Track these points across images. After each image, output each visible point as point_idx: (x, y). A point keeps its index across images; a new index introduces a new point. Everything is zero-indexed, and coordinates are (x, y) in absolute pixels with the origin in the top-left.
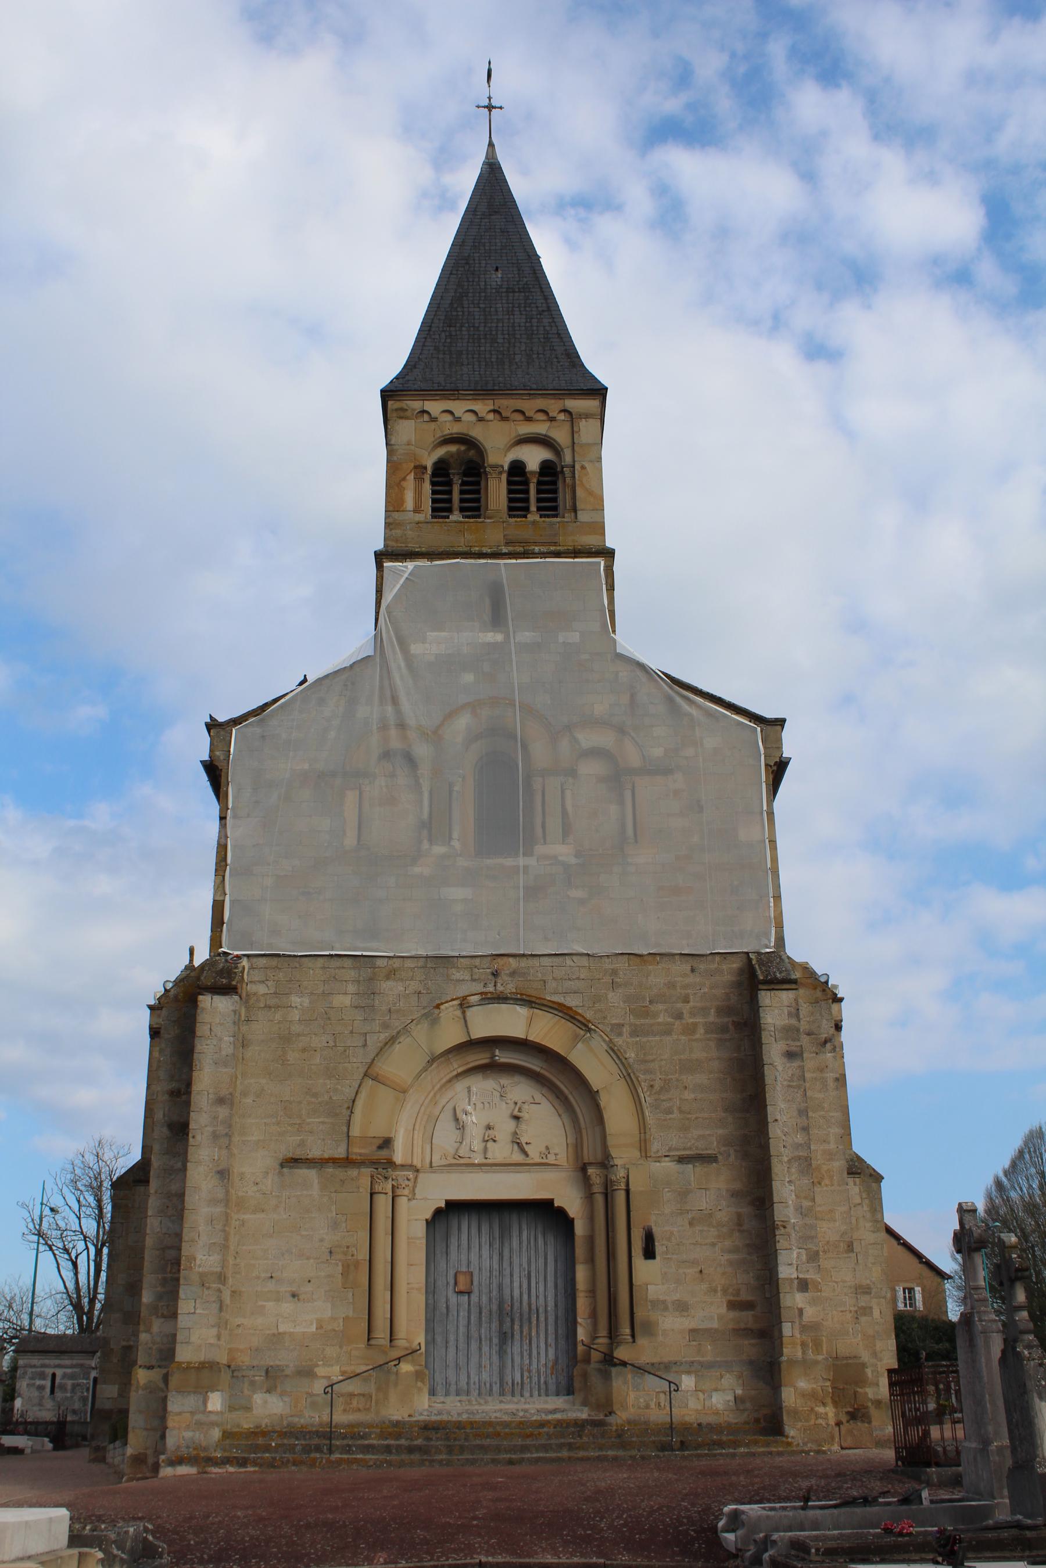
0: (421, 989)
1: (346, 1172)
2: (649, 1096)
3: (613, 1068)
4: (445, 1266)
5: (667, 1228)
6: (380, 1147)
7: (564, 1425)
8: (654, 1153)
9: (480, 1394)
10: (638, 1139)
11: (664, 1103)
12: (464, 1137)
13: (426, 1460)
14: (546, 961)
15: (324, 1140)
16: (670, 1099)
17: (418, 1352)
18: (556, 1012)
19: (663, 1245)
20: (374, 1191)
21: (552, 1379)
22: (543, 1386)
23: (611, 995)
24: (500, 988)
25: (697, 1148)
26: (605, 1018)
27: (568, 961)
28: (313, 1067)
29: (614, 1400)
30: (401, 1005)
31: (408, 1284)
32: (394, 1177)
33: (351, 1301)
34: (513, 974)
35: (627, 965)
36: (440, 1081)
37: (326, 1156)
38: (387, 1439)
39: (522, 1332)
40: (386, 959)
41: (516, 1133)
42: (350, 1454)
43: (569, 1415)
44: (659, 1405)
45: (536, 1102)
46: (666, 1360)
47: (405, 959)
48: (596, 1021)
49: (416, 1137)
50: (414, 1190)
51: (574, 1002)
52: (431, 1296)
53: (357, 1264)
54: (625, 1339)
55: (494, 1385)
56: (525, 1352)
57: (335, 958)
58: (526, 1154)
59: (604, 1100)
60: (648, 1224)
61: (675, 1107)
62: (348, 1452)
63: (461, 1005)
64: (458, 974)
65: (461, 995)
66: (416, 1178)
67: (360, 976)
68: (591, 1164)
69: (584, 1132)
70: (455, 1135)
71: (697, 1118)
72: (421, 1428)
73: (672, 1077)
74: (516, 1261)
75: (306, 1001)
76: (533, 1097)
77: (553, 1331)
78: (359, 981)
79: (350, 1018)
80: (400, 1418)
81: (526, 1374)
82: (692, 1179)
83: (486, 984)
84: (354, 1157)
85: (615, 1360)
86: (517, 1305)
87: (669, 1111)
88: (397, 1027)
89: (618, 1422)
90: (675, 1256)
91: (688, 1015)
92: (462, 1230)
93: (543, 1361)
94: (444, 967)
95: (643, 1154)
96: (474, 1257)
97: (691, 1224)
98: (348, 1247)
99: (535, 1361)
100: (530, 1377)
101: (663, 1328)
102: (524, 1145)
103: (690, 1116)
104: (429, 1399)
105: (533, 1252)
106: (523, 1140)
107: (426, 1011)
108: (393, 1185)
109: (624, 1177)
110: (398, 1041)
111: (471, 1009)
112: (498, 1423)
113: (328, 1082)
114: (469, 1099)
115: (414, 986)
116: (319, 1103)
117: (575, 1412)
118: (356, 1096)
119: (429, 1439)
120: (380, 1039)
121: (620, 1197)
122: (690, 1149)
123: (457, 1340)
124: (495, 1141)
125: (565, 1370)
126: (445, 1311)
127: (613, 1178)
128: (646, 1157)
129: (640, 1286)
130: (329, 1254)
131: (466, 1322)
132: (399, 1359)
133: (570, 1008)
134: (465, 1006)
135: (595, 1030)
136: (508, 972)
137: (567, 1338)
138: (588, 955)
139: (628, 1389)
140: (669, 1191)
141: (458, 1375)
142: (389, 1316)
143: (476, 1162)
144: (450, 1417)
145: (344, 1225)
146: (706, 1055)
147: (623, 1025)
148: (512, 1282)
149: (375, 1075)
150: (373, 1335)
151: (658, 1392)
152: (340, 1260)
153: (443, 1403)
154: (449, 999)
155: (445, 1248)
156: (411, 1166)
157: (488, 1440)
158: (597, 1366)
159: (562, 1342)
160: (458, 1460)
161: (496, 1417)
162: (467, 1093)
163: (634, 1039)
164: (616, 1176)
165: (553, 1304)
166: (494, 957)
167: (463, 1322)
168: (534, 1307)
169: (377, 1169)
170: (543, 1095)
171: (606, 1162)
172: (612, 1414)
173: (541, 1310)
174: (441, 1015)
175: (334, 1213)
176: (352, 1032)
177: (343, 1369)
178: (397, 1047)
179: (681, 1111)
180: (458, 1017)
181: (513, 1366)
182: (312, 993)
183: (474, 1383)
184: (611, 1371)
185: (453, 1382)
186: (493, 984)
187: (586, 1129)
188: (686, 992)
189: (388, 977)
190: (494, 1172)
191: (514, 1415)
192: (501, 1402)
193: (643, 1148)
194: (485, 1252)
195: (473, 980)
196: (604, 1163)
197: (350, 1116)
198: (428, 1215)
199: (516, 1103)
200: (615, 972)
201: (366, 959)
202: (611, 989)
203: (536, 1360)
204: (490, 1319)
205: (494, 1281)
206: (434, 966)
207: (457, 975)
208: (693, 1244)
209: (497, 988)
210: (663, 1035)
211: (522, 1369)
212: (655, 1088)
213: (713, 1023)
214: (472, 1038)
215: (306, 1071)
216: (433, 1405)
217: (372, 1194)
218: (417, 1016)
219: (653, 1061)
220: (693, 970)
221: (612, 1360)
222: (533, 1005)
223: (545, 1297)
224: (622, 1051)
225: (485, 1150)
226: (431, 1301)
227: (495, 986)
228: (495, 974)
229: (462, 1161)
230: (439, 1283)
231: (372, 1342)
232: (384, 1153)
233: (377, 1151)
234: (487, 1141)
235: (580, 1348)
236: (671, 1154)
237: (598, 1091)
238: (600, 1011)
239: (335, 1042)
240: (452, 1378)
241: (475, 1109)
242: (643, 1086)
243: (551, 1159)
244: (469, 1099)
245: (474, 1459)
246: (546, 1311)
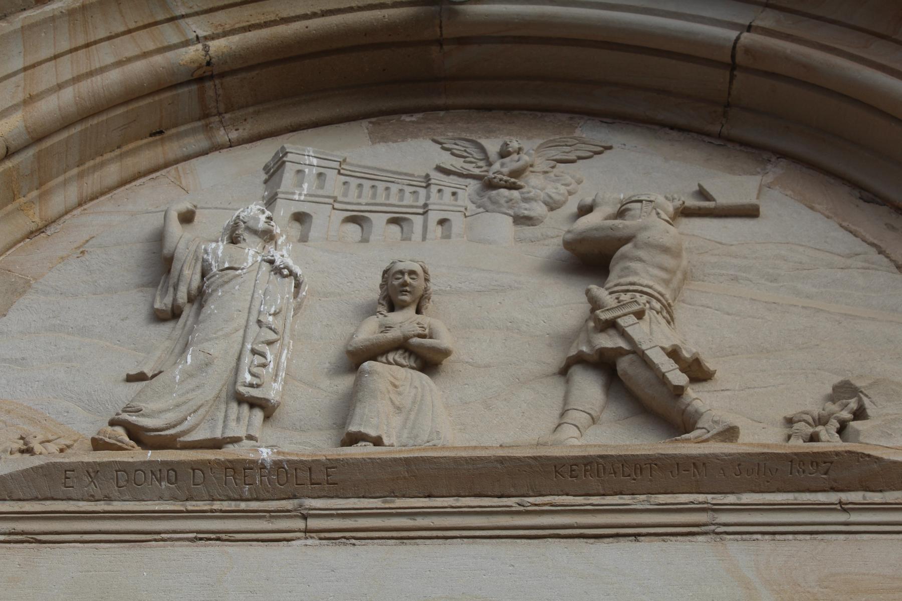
190: (403, 536)
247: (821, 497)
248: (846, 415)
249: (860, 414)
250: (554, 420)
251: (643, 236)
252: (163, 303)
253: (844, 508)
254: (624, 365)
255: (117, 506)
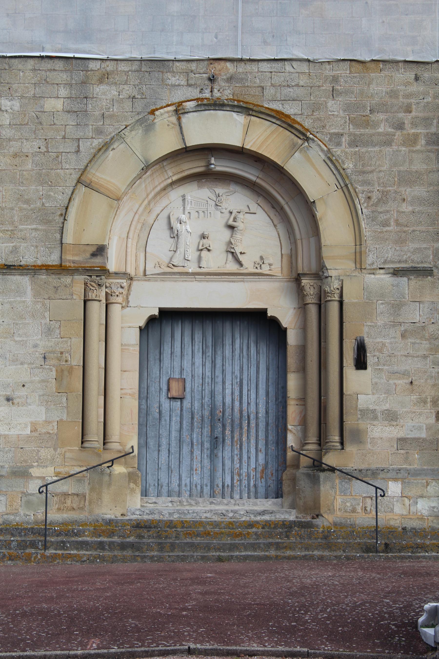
0: (135, 93)
1: (59, 279)
2: (365, 208)
3: (332, 180)
4: (158, 372)
5: (379, 340)
6: (94, 255)
7: (272, 526)
8: (370, 265)
9: (190, 496)
10: (354, 251)
11: (381, 215)
12: (179, 246)
13: (138, 556)
14: (265, 67)
15: (37, 247)
16: (388, 211)
17: (132, 455)
18: (274, 120)
19: (374, 356)
20: (87, 298)
21: (261, 482)
22: (252, 489)
23: (330, 103)
24: (217, 94)
25: (413, 261)
26: (324, 127)
27: (288, 67)
28: (24, 173)
29: (322, 503)
30: (115, 110)
31: (121, 389)
32: (108, 285)
33: (65, 405)
34: (230, 79)
35: (348, 72)
36: (153, 189)
37: (39, 263)
38: (100, 536)
39: (233, 437)
40: (99, 62)
41: (230, 243)
42: (66, 550)
43: (277, 516)
44: (366, 510)
45: (251, 212)
46: (373, 467)
47: (119, 62)
48: (314, 130)
49: (129, 245)
50: (127, 298)
51: (292, 110)
52: (144, 401)
53: (71, 370)
54: (333, 446)
55: (205, 487)
56: (235, 456)
57: (46, 60)
58: (241, 265)
59: (319, 212)
60: (361, 335)
61: (392, 220)
62: (63, 548)
63: (176, 111)
64: (174, 79)
65: (177, 101)
66: (130, 286)
67: (72, 79)
68: (304, 275)
69: (299, 242)
70: (170, 243)
71: (413, 231)
72: (133, 527)
73: (391, 188)
74: (228, 368)
75: (16, 105)
76: (248, 206)
77: (264, 437)
78: (71, 85)
79: (62, 123)
80: (113, 517)
81: (236, 477)
82: (407, 291)
83: (202, 89)
84: (68, 264)
85: (323, 465)
86: (228, 411)
87: (386, 224)
88: (110, 133)
89: (325, 524)
90: (386, 367)
91: (410, 125)
92: (175, 337)
93: (253, 466)
94: (159, 71)
95: (358, 266)
96: (187, 365)
97: (403, 336)
98: (62, 353)
99: (245, 465)
100: (240, 481)
101: (371, 436)
102: (239, 255)
103: (406, 229)
104: (142, 499)
105: (245, 360)
106: (238, 250)
107: (140, 117)
108: (106, 292)
109: (338, 289)
110: (112, 147)
111: (186, 115)
112: (208, 523)
113: (41, 188)
114: (184, 208)
115: (128, 90)
116: (31, 210)
117: (283, 514)
118: (69, 203)
119: (140, 537)
120: (94, 145)
121: (334, 308)
122: (406, 261)
123: (169, 444)
124: (209, 250)
125: (274, 474)
126: (157, 415)
127: (327, 289)
128: (361, 269)
129: (349, 395)
130: (43, 360)
131: (178, 427)
132: (112, 461)
133: (288, 116)
134: (180, 112)
135: (313, 140)
136: (225, 77)
137: (277, 443)
138: (309, 61)
139: (336, 493)
140: (382, 304)
141: (169, 477)
142: (102, 420)
143: (190, 271)
144: (161, 517)
145: (58, 331)
146: (426, 167)
147: (342, 135)
148: (224, 389)
149: (88, 182)
150: (86, 438)
151: (365, 497)
152: (54, 366)
153: (155, 503)
154: (164, 105)
155: (158, 355)
156: (125, 274)
157: (199, 538)
158: (305, 471)
159: (272, 447)
160: (169, 556)
161: (206, 518)
162: (181, 202)
163: (352, 150)
164: (330, 287)
165: (264, 411)
166: (212, 61)
167: (175, 426)
168: (245, 414)
169: (91, 276)
170: (259, 205)
171: (321, 273)
172: (319, 517)
173: (252, 416)
174: (155, 121)
175: (48, 320)
176: (64, 138)
177: (58, 470)
178: (111, 154)
179: (397, 223)
180: (173, 124)
181: (223, 470)
182: (22, 97)
183: (186, 485)
184: (319, 477)
185: (165, 484)
186: (209, 90)
187: (301, 239)
188: (409, 101)
189: (101, 81)
190: (207, 281)
191: (224, 515)
192: (211, 503)
193: (358, 260)
194: (198, 361)
195: (189, 85)
196: (318, 274)
197: (63, 223)
198: (142, 323)
199: (231, 213)
200: (335, 79)
201: (79, 61)
202: (332, 97)
203: (246, 465)
204: (202, 424)
205: (207, 387)
206: (148, 70)
207: (173, 80)
208: (405, 356)
209: (214, 94)
210: (384, 146)
211: (232, 473)
212: (372, 200)
213: (435, 134)
214: (188, 145)
215: (18, 177)
216: (145, 505)
217: (85, 302)
218: (130, 122)
219: (372, 172)
220: (417, 78)
221: (321, 466)
222: (251, 113)
223: (257, 404)
224: (340, 161)
225: (200, 259)
226: (144, 406)
227: (211, 91)
228: (212, 80)
229: (176, 270)
230: (152, 389)
231: (86, 445)
232: (97, 261)
233: (91, 258)
234: (202, 250)
235: (290, 454)
236: (386, 266)
237: (314, 202)
238: (319, 119)
239: (47, 147)
240: (164, 480)
241: (190, 218)
242: (360, 198)
243: (265, 269)
244: (184, 208)
245: (184, 556)
246: (257, 418)
247: (257, 277)
248: (261, 263)
249: (263, 263)
250: (225, 261)
251: (239, 228)
252: (172, 236)
253: (259, 278)
254: (234, 254)
255: (173, 276)
